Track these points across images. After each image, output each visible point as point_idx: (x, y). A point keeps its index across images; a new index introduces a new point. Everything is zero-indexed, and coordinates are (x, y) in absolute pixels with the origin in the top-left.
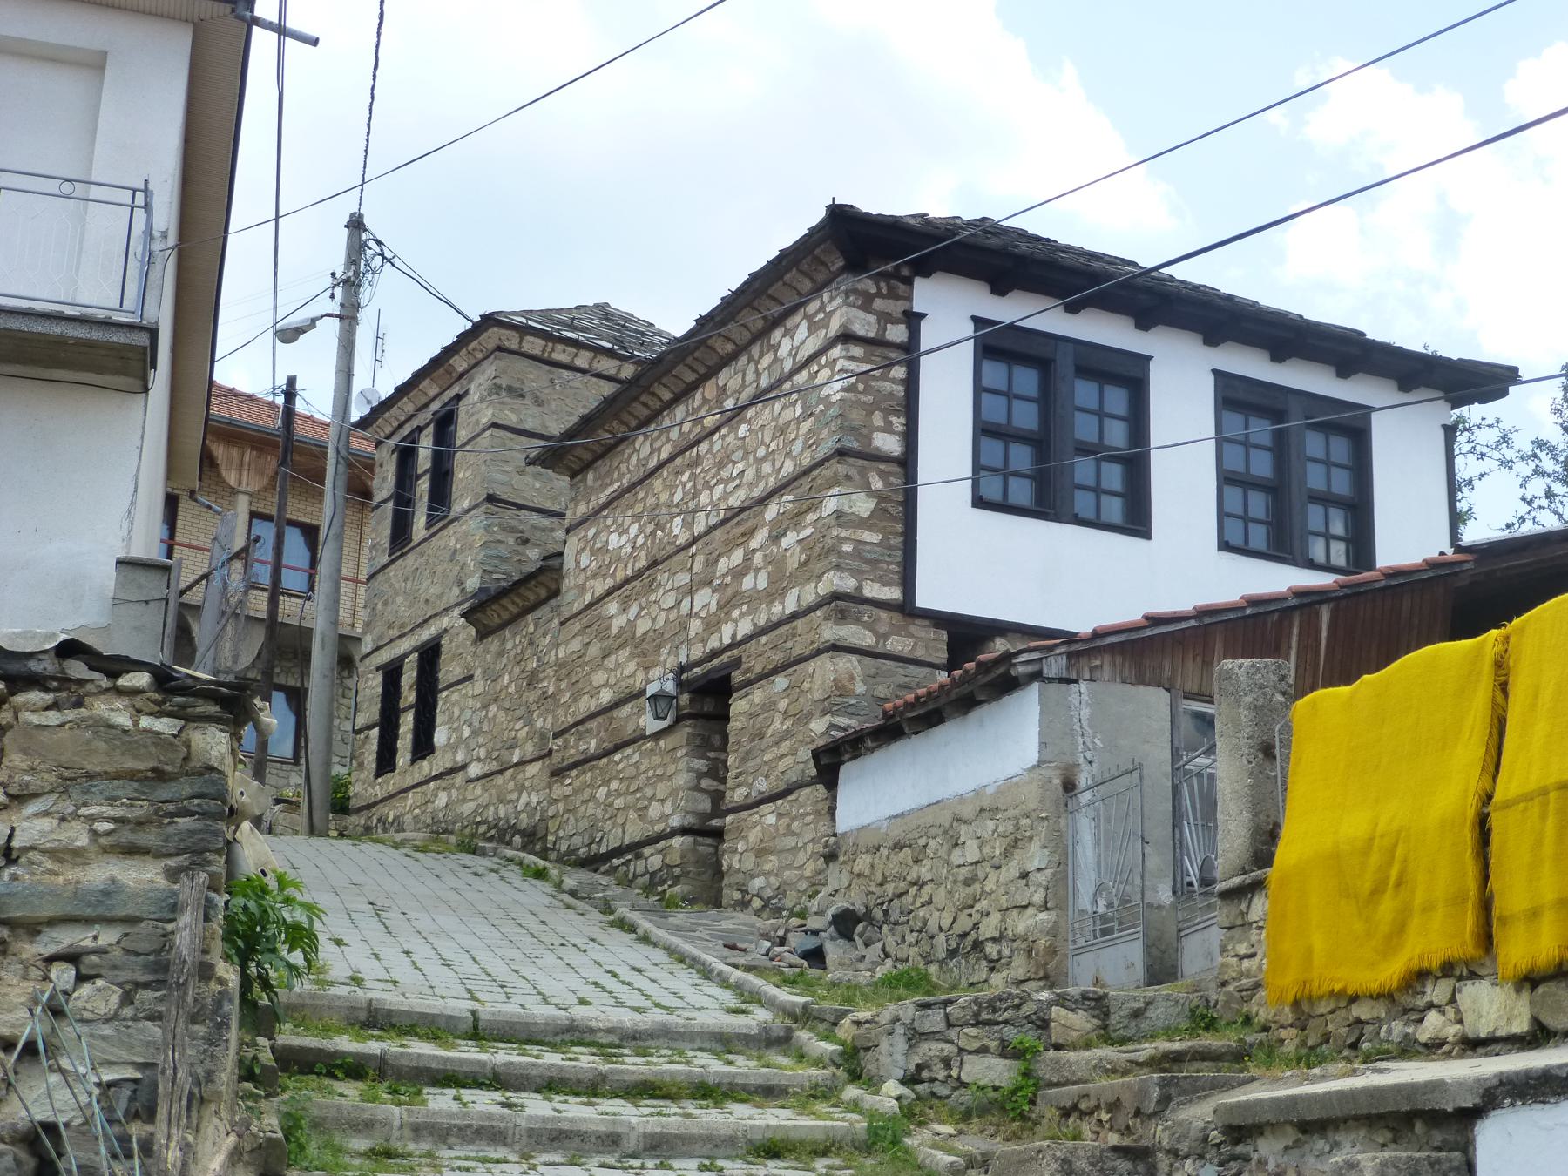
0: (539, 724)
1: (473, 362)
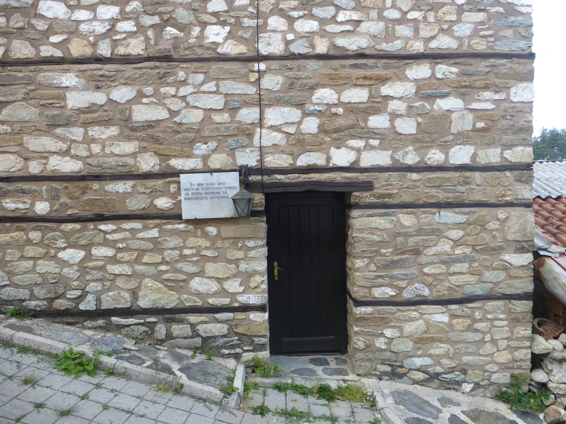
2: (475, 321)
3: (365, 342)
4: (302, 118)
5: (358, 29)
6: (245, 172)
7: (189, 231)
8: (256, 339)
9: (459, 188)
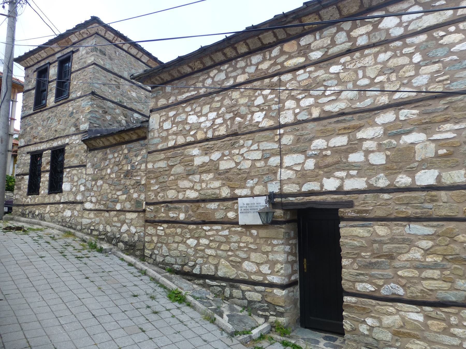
0: (135, 196)
1: (81, 38)
2: (451, 326)
3: (351, 325)
4: (305, 160)
5: (340, 97)
6: (271, 196)
7: (242, 232)
8: (278, 308)
9: (426, 205)
